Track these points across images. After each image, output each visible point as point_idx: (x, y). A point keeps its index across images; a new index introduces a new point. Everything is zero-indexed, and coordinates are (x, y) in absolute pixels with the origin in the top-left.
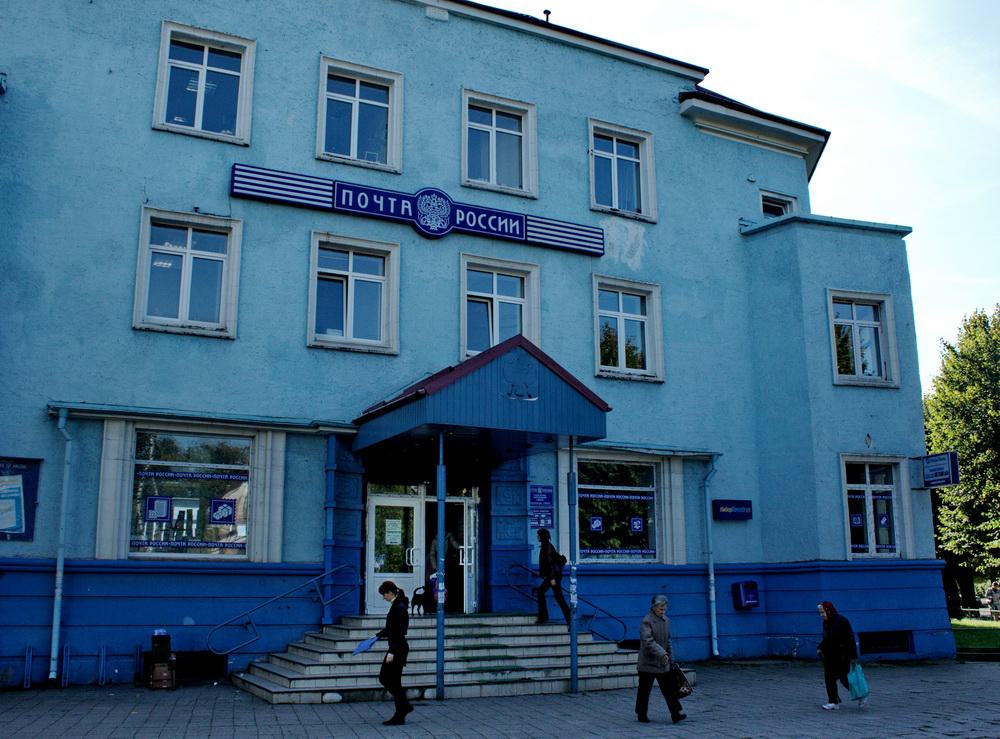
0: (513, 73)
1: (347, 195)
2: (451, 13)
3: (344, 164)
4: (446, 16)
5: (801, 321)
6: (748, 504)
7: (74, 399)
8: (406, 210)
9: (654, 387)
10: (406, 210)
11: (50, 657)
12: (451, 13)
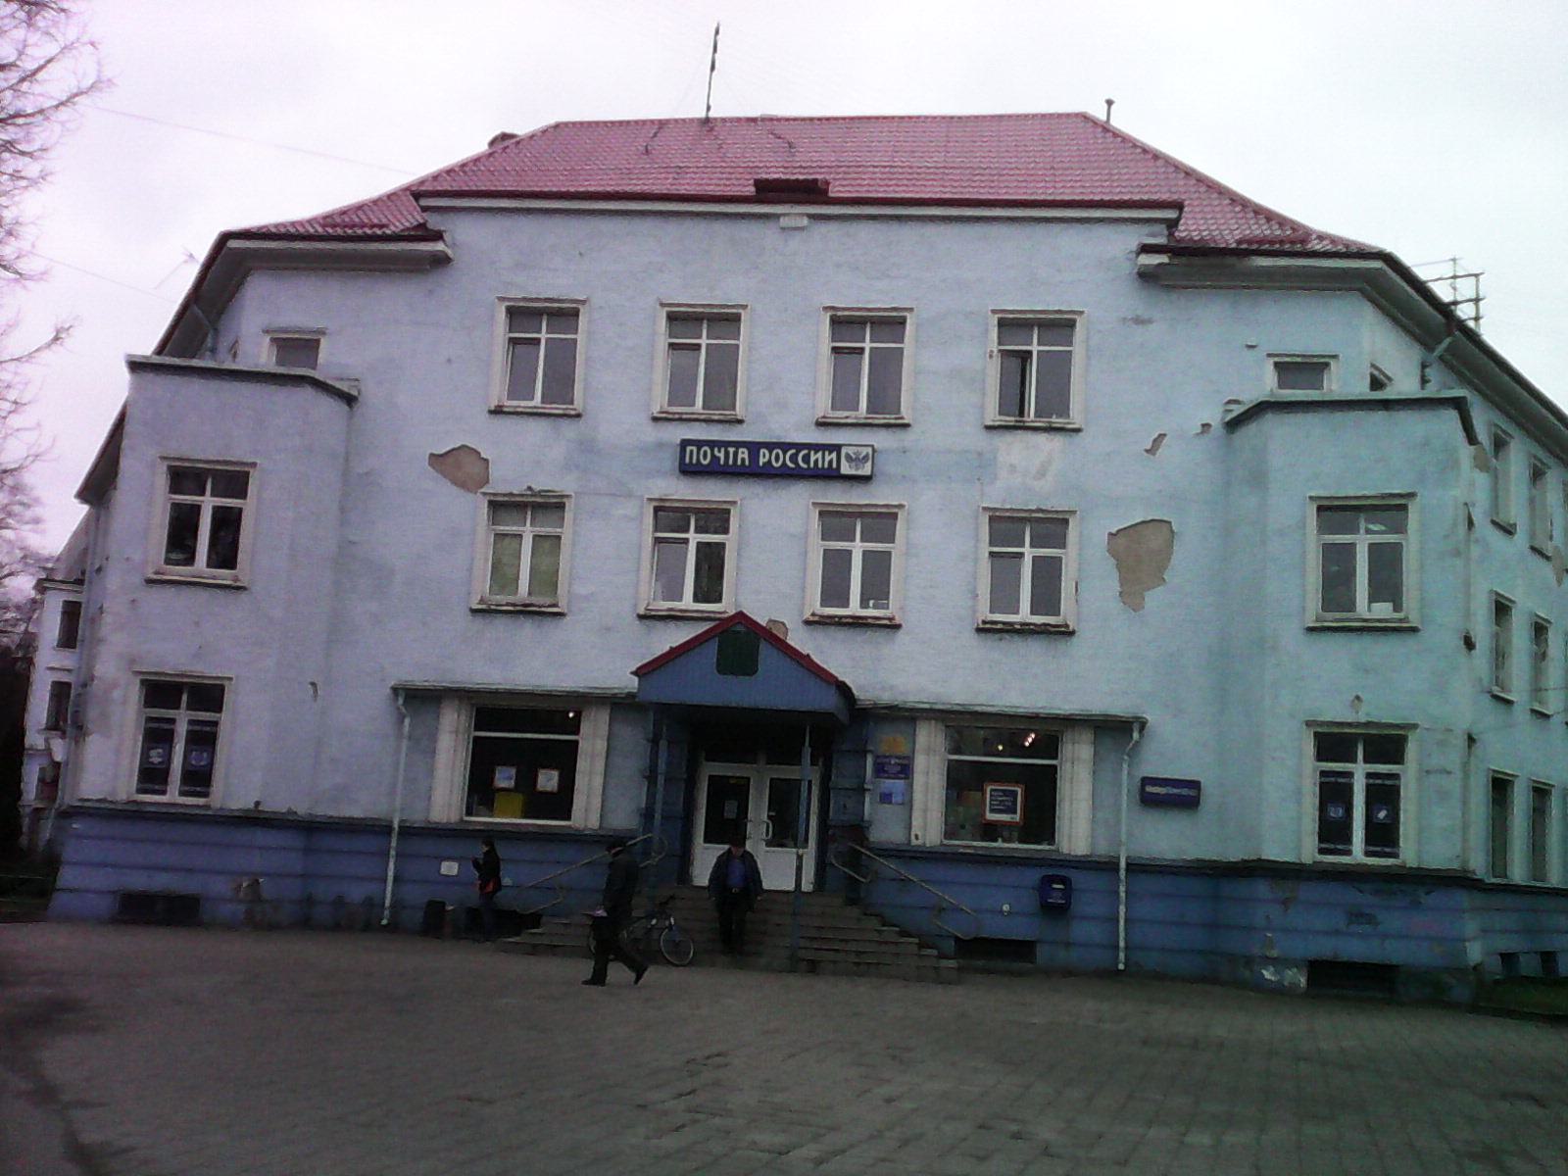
1: (692, 452)
2: (811, 216)
3: (680, 420)
4: (805, 221)
6: (1195, 785)
7: (420, 678)
8: (743, 460)
10: (743, 460)
12: (811, 216)
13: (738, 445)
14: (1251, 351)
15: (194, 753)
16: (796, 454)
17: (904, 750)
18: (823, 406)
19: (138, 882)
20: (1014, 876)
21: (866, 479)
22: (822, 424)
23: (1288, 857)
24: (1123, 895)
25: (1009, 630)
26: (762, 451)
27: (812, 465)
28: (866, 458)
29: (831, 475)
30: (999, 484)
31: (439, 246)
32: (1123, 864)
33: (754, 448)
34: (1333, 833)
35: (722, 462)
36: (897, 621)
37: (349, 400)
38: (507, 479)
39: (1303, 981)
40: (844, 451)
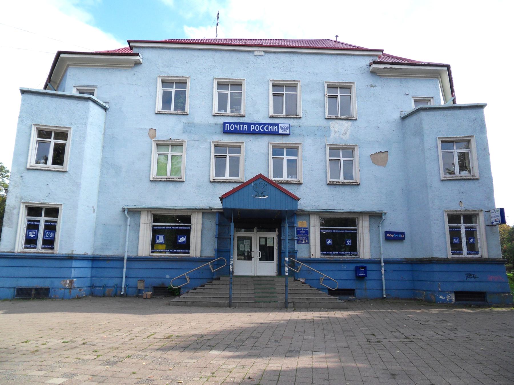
0: (291, 70)
1: (227, 126)
3: (223, 116)
4: (263, 53)
5: (424, 153)
6: (403, 233)
7: (132, 204)
8: (245, 128)
9: (356, 187)
10: (245, 128)
11: (122, 287)
13: (243, 124)
14: (407, 96)
15: (47, 233)
16: (264, 126)
17: (306, 226)
18: (272, 112)
19: (24, 283)
20: (345, 267)
21: (288, 135)
22: (272, 117)
23: (443, 256)
24: (383, 272)
25: (338, 184)
26: (252, 126)
27: (269, 131)
28: (287, 128)
29: (276, 134)
30: (331, 137)
31: (138, 58)
32: (382, 262)
33: (249, 125)
34: (456, 247)
35: (238, 130)
36: (301, 182)
37: (105, 109)
38: (162, 136)
39: (454, 299)
40: (280, 125)
